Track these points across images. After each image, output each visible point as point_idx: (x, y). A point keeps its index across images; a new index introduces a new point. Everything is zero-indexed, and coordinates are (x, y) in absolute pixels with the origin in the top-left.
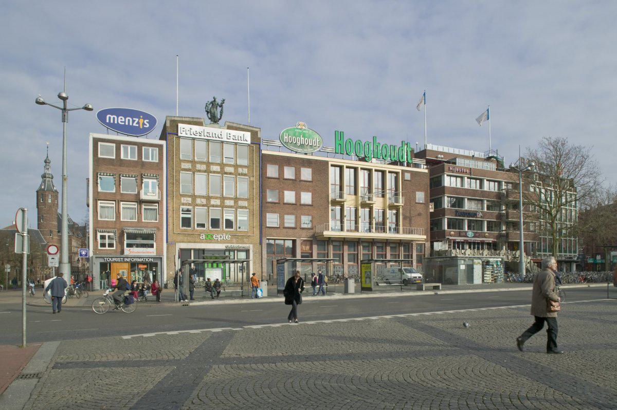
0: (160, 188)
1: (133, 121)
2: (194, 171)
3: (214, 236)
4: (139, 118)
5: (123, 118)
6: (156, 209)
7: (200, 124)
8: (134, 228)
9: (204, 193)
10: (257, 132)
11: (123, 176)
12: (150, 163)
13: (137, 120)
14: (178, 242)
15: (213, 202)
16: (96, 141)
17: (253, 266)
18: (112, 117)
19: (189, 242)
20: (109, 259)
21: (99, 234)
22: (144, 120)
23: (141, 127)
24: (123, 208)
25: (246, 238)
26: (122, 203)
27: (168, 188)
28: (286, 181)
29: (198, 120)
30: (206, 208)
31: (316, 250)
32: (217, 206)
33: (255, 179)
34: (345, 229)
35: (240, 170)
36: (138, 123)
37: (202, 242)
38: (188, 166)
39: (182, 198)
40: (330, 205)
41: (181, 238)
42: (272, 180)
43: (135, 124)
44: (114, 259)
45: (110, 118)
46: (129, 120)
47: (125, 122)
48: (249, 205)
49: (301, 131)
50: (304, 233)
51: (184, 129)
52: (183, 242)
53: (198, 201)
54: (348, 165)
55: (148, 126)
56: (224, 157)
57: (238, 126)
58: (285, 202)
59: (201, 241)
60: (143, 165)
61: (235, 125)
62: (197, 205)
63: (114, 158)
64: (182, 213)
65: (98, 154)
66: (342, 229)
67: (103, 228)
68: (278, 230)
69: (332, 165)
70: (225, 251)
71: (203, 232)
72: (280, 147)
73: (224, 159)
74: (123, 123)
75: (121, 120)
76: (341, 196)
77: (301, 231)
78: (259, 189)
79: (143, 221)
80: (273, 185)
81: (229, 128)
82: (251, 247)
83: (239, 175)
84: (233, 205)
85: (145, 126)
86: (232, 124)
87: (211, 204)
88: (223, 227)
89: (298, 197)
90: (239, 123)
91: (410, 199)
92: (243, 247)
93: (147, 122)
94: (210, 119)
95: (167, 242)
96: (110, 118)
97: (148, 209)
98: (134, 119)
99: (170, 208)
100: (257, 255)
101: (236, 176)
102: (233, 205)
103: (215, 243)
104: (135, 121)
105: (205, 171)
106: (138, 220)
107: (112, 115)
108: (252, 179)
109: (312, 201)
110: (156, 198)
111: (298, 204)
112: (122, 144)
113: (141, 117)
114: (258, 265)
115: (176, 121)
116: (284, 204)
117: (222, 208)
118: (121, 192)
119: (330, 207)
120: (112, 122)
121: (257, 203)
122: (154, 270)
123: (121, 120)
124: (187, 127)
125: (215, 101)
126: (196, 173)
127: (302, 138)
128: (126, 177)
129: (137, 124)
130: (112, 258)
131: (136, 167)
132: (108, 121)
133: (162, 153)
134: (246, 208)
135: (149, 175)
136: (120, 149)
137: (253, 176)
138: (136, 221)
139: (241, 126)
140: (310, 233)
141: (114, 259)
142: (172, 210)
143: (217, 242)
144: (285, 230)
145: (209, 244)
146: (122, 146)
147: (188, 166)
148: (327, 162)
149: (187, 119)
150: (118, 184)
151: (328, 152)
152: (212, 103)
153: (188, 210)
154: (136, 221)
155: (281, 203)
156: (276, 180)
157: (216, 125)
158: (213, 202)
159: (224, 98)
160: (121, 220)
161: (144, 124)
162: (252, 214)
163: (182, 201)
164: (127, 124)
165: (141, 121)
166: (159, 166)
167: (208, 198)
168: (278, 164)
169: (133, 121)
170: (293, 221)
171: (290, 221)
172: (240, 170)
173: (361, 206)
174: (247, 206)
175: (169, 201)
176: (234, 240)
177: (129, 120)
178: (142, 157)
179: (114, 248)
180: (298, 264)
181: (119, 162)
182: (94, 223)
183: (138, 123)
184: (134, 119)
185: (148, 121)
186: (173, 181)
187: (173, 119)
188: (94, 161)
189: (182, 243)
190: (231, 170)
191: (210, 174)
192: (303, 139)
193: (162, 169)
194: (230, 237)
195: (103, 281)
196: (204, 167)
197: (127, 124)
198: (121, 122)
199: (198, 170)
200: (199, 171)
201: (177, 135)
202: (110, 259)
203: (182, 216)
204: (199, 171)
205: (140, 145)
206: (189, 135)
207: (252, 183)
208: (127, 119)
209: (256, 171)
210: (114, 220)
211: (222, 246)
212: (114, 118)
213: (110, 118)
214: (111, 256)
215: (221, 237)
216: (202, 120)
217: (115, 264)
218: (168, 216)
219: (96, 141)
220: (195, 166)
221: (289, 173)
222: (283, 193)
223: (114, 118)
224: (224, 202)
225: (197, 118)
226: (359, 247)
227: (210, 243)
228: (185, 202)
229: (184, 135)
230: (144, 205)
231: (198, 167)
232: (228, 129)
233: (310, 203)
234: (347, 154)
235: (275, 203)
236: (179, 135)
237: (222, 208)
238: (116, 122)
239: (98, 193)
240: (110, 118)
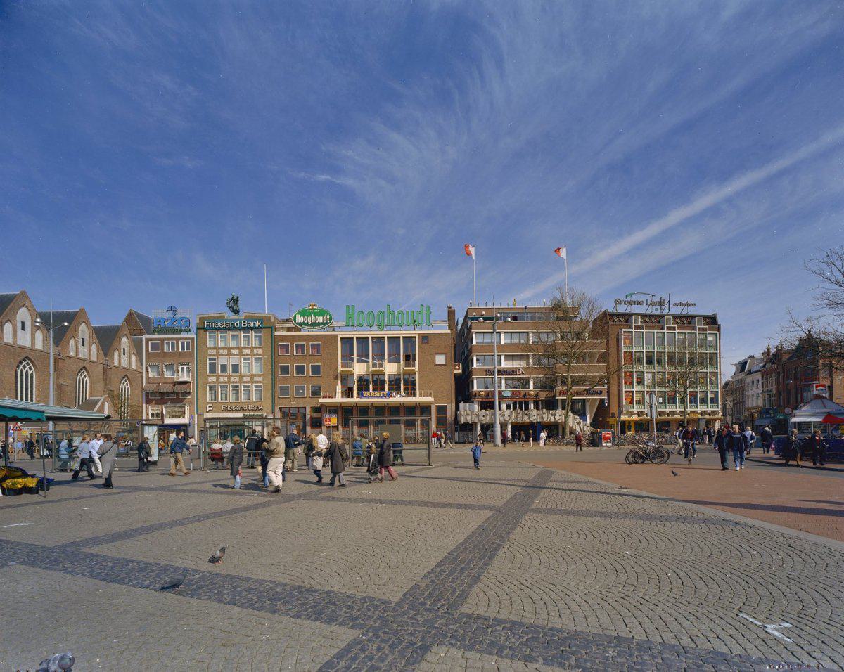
35: (255, 351)
48: (263, 380)
54: (357, 336)
69: (341, 338)
91: (428, 364)
110: (189, 380)
134: (260, 382)
166: (191, 354)
172: (255, 351)
181: (165, 355)
188: (146, 355)
190: (248, 351)
196: (225, 352)
200: (222, 355)
204: (222, 355)
211: (240, 415)
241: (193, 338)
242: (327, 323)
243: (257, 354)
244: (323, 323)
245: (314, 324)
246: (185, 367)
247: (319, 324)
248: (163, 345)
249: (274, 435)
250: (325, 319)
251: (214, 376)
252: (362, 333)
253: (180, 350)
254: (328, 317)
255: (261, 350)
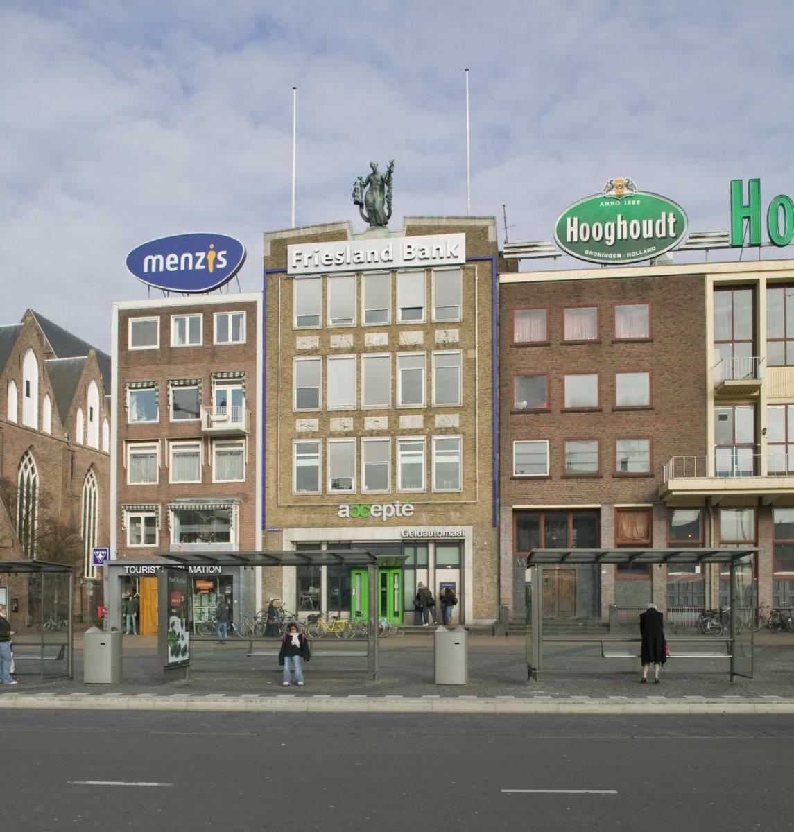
0: (251, 406)
1: (196, 259)
2: (324, 352)
3: (372, 509)
4: (207, 251)
5: (175, 256)
6: (242, 452)
7: (340, 236)
8: (187, 499)
9: (351, 405)
10: (484, 230)
11: (130, 388)
12: (230, 346)
13: (202, 255)
14: (287, 527)
15: (370, 423)
16: (124, 316)
17: (474, 582)
18: (154, 259)
19: (313, 526)
20: (133, 569)
21: (127, 516)
22: (217, 250)
23: (211, 270)
24: (174, 454)
25: (456, 510)
26: (172, 444)
27: (267, 401)
28: (570, 349)
29: (336, 228)
30: (353, 439)
31: (664, 536)
32: (380, 433)
33: (480, 354)
34: (764, 471)
35: (440, 336)
36: (205, 262)
37: (344, 526)
38: (311, 342)
39: (298, 422)
40: (710, 403)
41: (294, 516)
42: (529, 349)
43: (198, 266)
44: (142, 569)
45: (150, 261)
46: (187, 259)
47: (178, 265)
49: (618, 203)
50: (626, 488)
51: (300, 257)
52: (298, 526)
53: (336, 424)
55: (225, 262)
56: (399, 306)
57: (435, 223)
58: (568, 404)
59: (342, 523)
60: (211, 353)
61: (426, 222)
62: (332, 435)
63: (158, 347)
64: (298, 458)
65: (127, 345)
66: (757, 471)
67: (134, 501)
68: (544, 486)
69: (719, 287)
70: (405, 544)
71: (345, 500)
72: (555, 257)
73: (399, 312)
74: (176, 269)
75: (170, 262)
76: (755, 374)
77: (616, 484)
78: (490, 379)
79: (214, 481)
80: (532, 365)
81: (411, 231)
82: (467, 532)
83: (438, 347)
84: (421, 426)
85: (219, 266)
86: (417, 223)
87: (366, 429)
88: (394, 484)
89: (607, 389)
90: (436, 215)
92: (447, 534)
93: (223, 256)
94: (367, 220)
95: (264, 528)
96: (152, 261)
97: (225, 453)
98: (197, 254)
99: (271, 447)
100: (486, 554)
101: (429, 351)
102: (421, 426)
103: (376, 525)
104: (199, 257)
105: (352, 350)
106: (203, 479)
107: (154, 255)
108: (471, 354)
109: (652, 397)
110: (242, 426)
111: (607, 408)
112: (174, 313)
113: (212, 246)
114: (488, 582)
115: (285, 240)
116: (565, 411)
117: (394, 436)
118: (172, 420)
119: (712, 411)
120: (154, 270)
121: (483, 419)
122: (228, 592)
123: (170, 262)
124: (307, 248)
125: (375, 172)
126: (329, 357)
127: (620, 223)
128: (185, 385)
129: (201, 264)
130: (139, 565)
131: (199, 361)
132: (146, 270)
133: (255, 321)
134: (454, 431)
135: (231, 376)
136: (169, 327)
137: (475, 348)
138: (200, 482)
139: (444, 222)
140: (646, 487)
141: (142, 569)
142: (274, 450)
143: (380, 523)
144: (566, 484)
145: (360, 529)
146: (173, 319)
147: (311, 342)
148: (700, 278)
149: (310, 232)
150: (165, 402)
151: (707, 249)
152: (369, 180)
153: (314, 448)
154: (200, 482)
155: (556, 408)
156: (540, 349)
157: (380, 232)
158: (370, 423)
159: (391, 160)
160: (171, 482)
161: (217, 261)
162: (470, 447)
163: (299, 429)
164: (182, 268)
165: (211, 255)
167: (359, 415)
168: (544, 307)
169: (196, 259)
170: (595, 457)
171: (584, 456)
172: (440, 336)
173: (716, 399)
174: (457, 425)
175: (269, 431)
176: (424, 517)
177: (187, 259)
178: (213, 338)
179: (156, 545)
180: (607, 572)
181: (169, 355)
182: (119, 493)
183: (205, 262)
184: (197, 254)
185: (224, 252)
186: (277, 380)
187: (278, 236)
189: (295, 529)
190: (417, 337)
191: (364, 355)
192: (625, 223)
193: (253, 358)
194: (412, 508)
195: (128, 616)
197: (182, 268)
198: (172, 266)
199: (336, 349)
200: (338, 351)
201: (285, 272)
202: (136, 569)
203: (297, 463)
204: (338, 351)
205: (208, 310)
206: (312, 269)
207: (470, 364)
208: (184, 256)
209: (482, 332)
210: (157, 483)
212: (158, 261)
213: (150, 261)
214: (137, 563)
215: (389, 510)
216: (345, 227)
217: (147, 579)
218: (267, 468)
219: (124, 316)
220: (329, 341)
221: (579, 326)
222: (562, 381)
223: (158, 261)
224: (397, 422)
225: (333, 224)
226: (707, 523)
227: (362, 526)
228: (304, 429)
229: (300, 269)
230: (217, 446)
231: (337, 341)
232: (408, 235)
233: (645, 401)
234: (773, 243)
235: (537, 412)
236: (290, 271)
237: (394, 436)
238: (161, 269)
239: (127, 426)
240: (152, 261)
241: (250, 307)
242: (667, 240)
243: (446, 345)
244: (652, 241)
245: (623, 245)
246: (229, 389)
247: (642, 243)
248: (166, 327)
249: (616, 604)
250: (663, 225)
251: (314, 415)
252: (780, 265)
253: (215, 342)
254: (672, 220)
255: (456, 331)
